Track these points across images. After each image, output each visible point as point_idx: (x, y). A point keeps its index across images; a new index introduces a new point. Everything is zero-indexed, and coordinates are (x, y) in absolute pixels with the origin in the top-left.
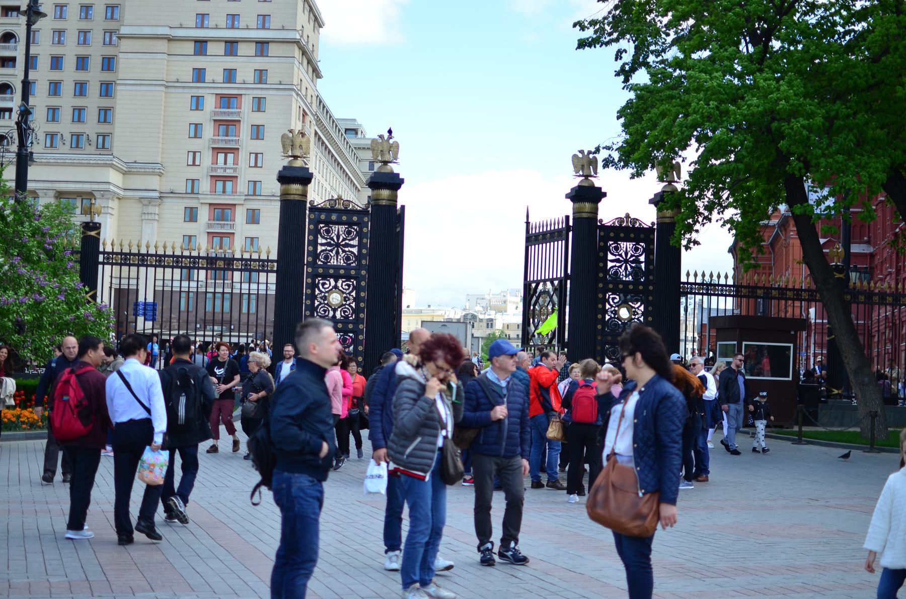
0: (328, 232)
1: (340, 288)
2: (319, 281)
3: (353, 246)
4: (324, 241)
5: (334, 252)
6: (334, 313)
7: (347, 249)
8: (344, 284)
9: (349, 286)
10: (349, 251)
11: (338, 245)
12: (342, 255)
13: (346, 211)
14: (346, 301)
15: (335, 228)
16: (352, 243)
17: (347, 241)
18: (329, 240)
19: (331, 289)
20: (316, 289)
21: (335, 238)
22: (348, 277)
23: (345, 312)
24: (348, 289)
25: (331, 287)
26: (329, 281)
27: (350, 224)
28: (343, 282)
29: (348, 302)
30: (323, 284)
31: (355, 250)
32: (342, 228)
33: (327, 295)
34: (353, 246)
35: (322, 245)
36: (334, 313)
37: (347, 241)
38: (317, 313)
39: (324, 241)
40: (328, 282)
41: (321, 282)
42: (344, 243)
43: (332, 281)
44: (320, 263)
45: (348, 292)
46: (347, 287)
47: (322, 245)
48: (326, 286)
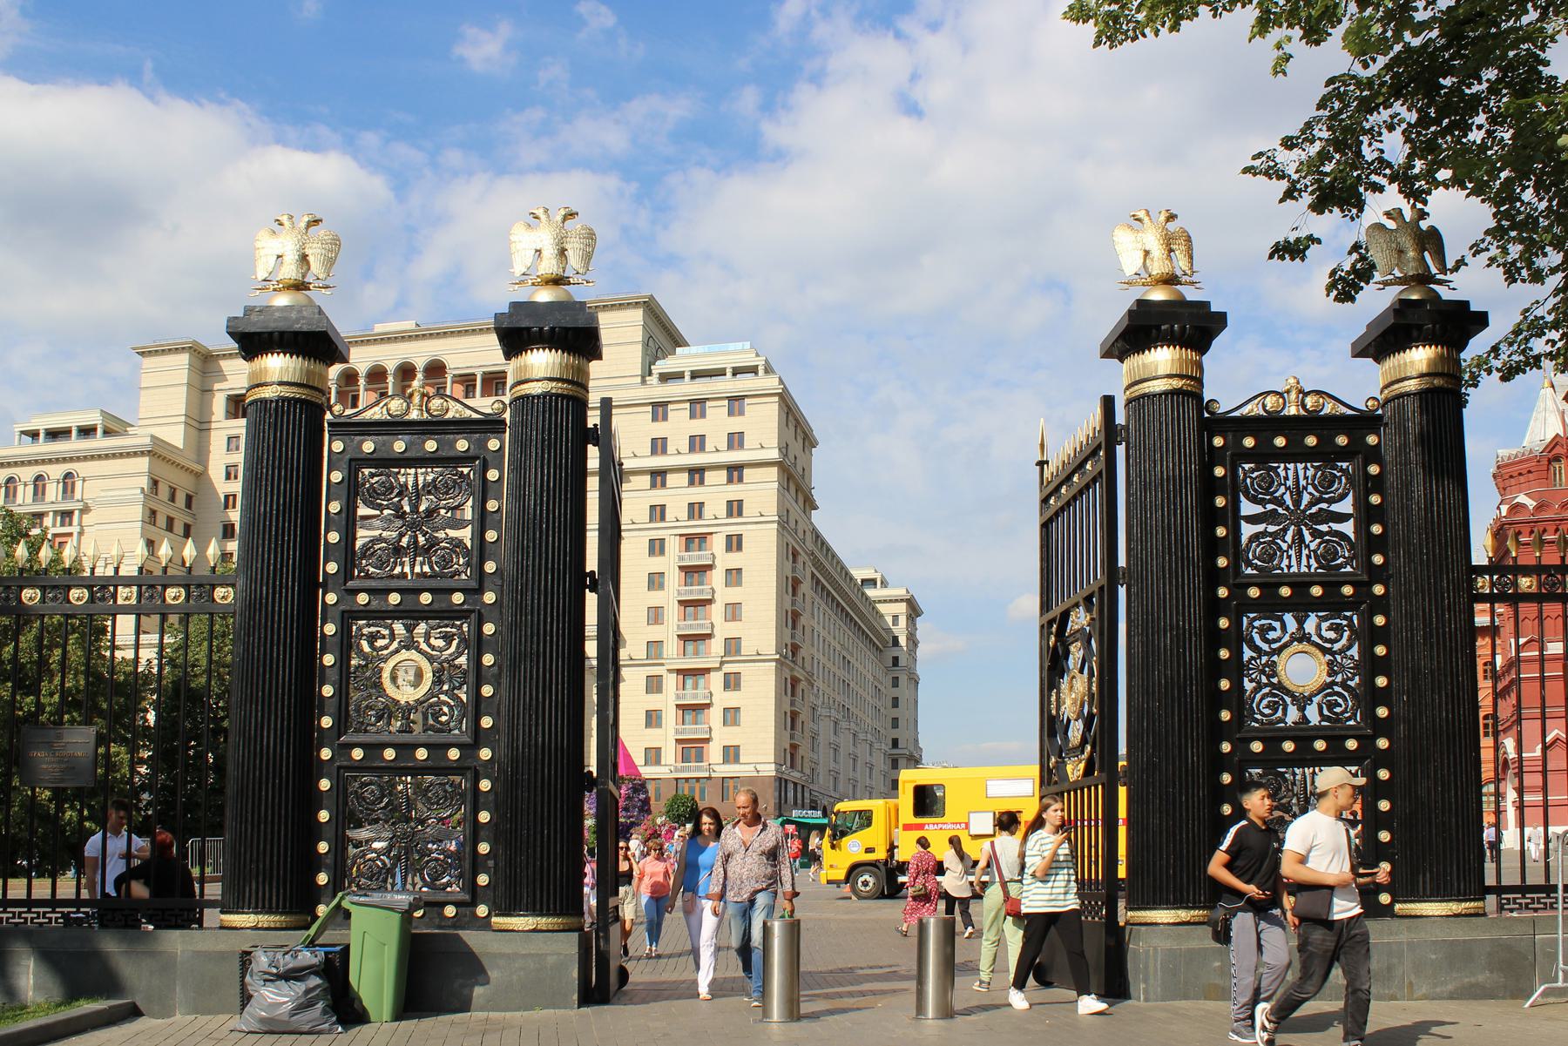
0: (1268, 484)
3: (1342, 518)
4: (1258, 509)
6: (1302, 709)
7: (1324, 528)
8: (1325, 625)
9: (1338, 629)
11: (1299, 518)
12: (1313, 546)
13: (1312, 422)
15: (1289, 471)
16: (1335, 508)
17: (1324, 506)
18: (1270, 507)
20: (1245, 648)
22: (1332, 605)
23: (1331, 706)
25: (1287, 638)
27: (1325, 455)
30: (1263, 631)
31: (1348, 528)
32: (1303, 472)
33: (1275, 658)
34: (1342, 518)
35: (1252, 520)
36: (1302, 709)
37: (1324, 506)
39: (1258, 509)
40: (1277, 624)
41: (1257, 624)
42: (1314, 510)
44: (1249, 571)
45: (1337, 647)
46: (1331, 635)
47: (1252, 520)
48: (1272, 635)
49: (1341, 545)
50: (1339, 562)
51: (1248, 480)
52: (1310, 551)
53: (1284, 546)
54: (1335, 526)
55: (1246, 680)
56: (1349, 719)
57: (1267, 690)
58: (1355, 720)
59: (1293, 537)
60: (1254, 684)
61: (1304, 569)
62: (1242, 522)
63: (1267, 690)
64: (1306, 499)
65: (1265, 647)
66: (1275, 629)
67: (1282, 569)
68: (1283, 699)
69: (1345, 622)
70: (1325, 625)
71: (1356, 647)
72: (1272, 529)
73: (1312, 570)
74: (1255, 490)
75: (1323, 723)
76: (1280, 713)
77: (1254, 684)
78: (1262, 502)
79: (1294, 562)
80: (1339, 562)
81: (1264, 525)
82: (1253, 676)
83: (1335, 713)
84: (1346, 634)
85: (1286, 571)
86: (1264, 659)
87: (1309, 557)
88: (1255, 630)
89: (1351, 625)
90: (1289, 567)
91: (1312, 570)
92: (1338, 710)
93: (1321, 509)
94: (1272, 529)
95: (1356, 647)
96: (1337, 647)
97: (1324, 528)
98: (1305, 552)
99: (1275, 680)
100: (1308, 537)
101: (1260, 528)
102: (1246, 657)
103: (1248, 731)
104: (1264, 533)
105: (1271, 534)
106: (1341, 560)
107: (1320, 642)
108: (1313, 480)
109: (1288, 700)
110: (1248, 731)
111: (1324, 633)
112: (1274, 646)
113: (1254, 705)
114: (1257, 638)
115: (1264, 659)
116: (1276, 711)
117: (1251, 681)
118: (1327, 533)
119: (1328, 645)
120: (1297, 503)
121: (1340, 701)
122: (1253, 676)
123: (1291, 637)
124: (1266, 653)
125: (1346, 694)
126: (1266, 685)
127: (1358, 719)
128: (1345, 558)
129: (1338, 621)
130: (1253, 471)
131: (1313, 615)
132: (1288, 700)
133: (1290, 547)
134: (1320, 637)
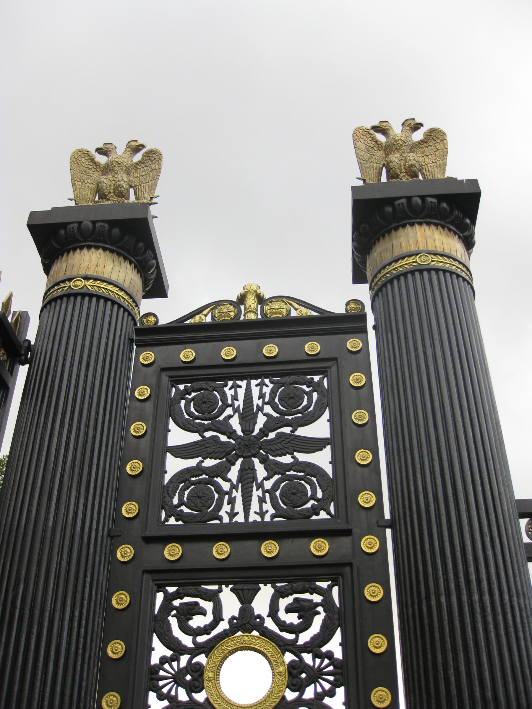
1: (270, 624)
2: (169, 598)
5: (233, 474)
7: (287, 459)
8: (284, 602)
10: (297, 465)
14: (299, 687)
17: (287, 430)
19: (225, 635)
20: (156, 642)
21: (235, 423)
25: (223, 626)
26: (214, 597)
28: (279, 594)
29: (309, 693)
33: (201, 659)
37: (287, 430)
41: (176, 603)
42: (272, 435)
44: (172, 521)
45: (304, 638)
46: (293, 619)
48: (197, 622)
49: (310, 483)
50: (308, 505)
51: (183, 403)
52: (264, 492)
53: (226, 486)
54: (302, 457)
61: (253, 517)
62: (168, 455)
64: (261, 420)
65: (187, 641)
66: (203, 613)
67: (220, 518)
69: (317, 598)
70: (284, 602)
71: (338, 637)
72: (209, 463)
73: (267, 518)
74: (190, 414)
78: (200, 430)
79: (239, 507)
80: (308, 505)
81: (200, 458)
85: (226, 520)
87: (262, 500)
88: (174, 612)
89: (327, 604)
90: (232, 514)
91: (267, 518)
94: (209, 463)
95: (338, 637)
96: (304, 638)
97: (287, 459)
98: (256, 493)
100: (261, 472)
101: (193, 463)
104: (199, 470)
108: (272, 397)
111: (282, 615)
112: (201, 639)
114: (173, 622)
115: (184, 659)
118: (289, 467)
119: (291, 637)
120: (247, 430)
122: (165, 690)
123: (230, 622)
128: (317, 500)
129: (306, 596)
130: (187, 391)
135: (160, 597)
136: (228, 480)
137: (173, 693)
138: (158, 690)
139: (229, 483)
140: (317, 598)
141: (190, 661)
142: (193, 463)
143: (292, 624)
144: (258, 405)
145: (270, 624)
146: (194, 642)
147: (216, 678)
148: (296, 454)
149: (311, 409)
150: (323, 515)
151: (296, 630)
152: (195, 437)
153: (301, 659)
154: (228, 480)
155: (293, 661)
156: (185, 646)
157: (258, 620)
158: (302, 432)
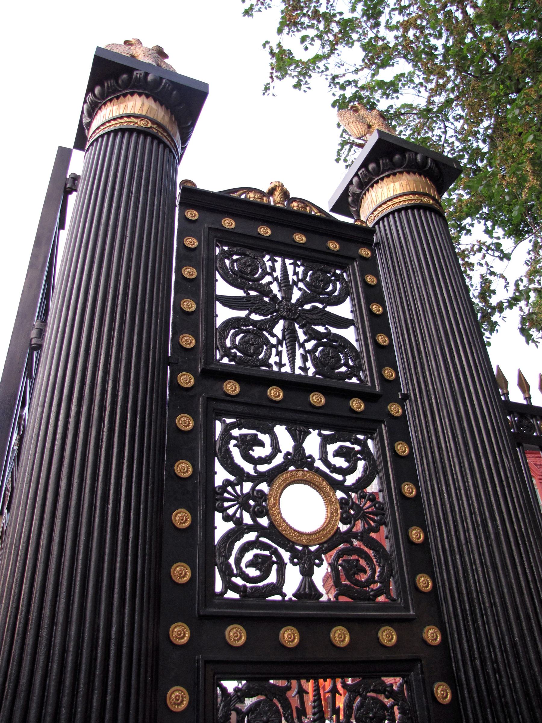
1: (319, 464)
2: (227, 428)
6: (307, 573)
7: (321, 329)
8: (332, 448)
19: (281, 469)
20: (218, 467)
24: (352, 470)
25: (279, 460)
36: (307, 573)
38: (227, 574)
40: (265, 438)
41: (236, 432)
42: (307, 307)
43: (281, 431)
44: (226, 360)
45: (351, 480)
46: (341, 462)
48: (258, 452)
54: (334, 330)
55: (218, 516)
56: (379, 593)
57: (251, 536)
58: (388, 594)
59: (283, 330)
60: (231, 525)
63: (251, 536)
67: (270, 366)
68: (275, 552)
69: (357, 448)
75: (342, 599)
76: (272, 578)
77: (231, 525)
79: (285, 359)
82: (231, 512)
83: (358, 583)
84: (361, 464)
86: (247, 487)
88: (233, 442)
92: (363, 578)
93: (315, 308)
94: (255, 317)
97: (321, 329)
98: (299, 352)
99: (264, 521)
101: (243, 314)
102: (218, 481)
103: (219, 606)
104: (247, 321)
105: (254, 323)
106: (343, 369)
107: (327, 471)
109: (286, 555)
110: (219, 606)
112: (263, 468)
113: (232, 560)
116: (265, 574)
117: (227, 518)
119: (339, 477)
121: (363, 563)
124: (249, 478)
125: (371, 553)
126: (249, 529)
127: (393, 594)
131: (314, 433)
132: (286, 555)
133: (280, 342)
134: (324, 460)
135: (219, 427)
136: (274, 335)
137: (238, 515)
138: (223, 510)
139: (275, 338)
140: (357, 448)
141: (253, 489)
142: (243, 314)
143: (341, 467)
144: (293, 280)
145: (319, 464)
146: (256, 471)
147: (277, 504)
148: (327, 326)
149: (336, 293)
150: (354, 380)
151: (345, 472)
152: (240, 293)
153: (253, 518)
154: (274, 335)
155: (342, 499)
156: (248, 473)
157: (309, 460)
158: (329, 309)
